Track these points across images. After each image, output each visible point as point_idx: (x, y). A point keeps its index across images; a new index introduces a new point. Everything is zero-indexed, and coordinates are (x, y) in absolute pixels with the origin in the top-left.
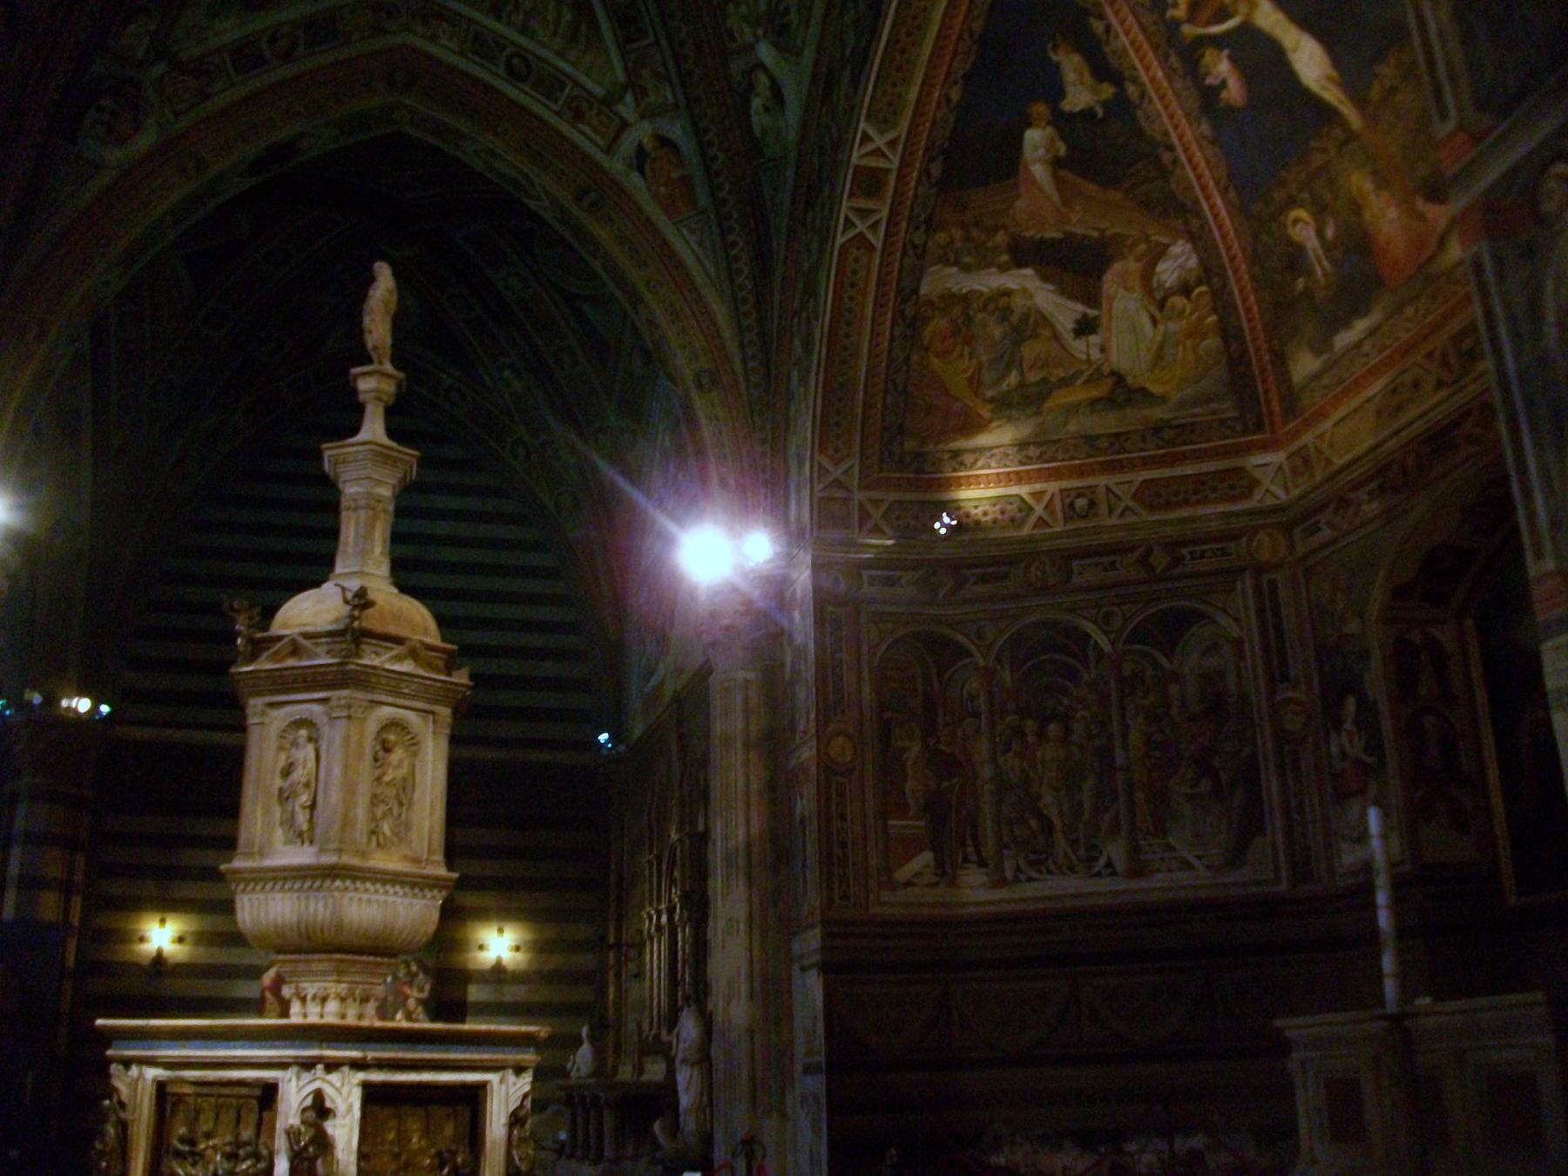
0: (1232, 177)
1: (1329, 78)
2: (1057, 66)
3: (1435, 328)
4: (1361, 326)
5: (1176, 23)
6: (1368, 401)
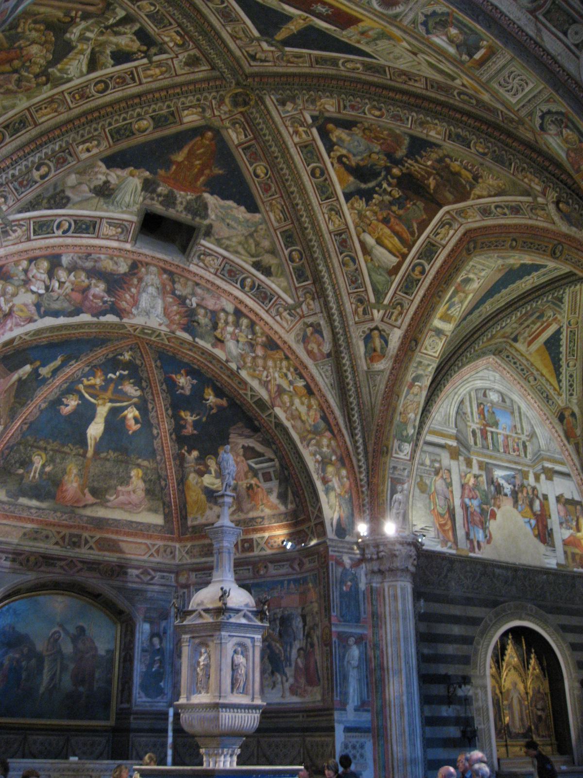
0: (31, 423)
1: (95, 439)
2: (56, 359)
3: (67, 527)
4: (34, 503)
5: (82, 382)
6: (23, 527)
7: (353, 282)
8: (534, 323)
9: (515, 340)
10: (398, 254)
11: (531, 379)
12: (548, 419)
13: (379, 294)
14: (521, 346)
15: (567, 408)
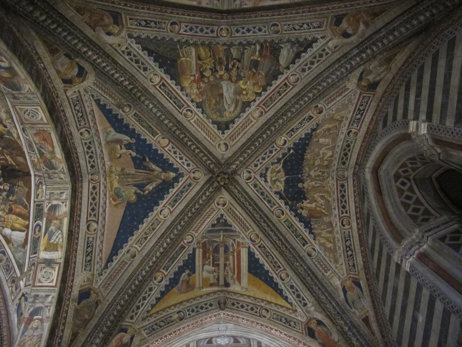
7: (7, 270)
8: (227, 259)
9: (227, 285)
10: (24, 229)
11: (264, 313)
12: (300, 342)
13: (21, 267)
14: (234, 287)
15: (310, 320)
